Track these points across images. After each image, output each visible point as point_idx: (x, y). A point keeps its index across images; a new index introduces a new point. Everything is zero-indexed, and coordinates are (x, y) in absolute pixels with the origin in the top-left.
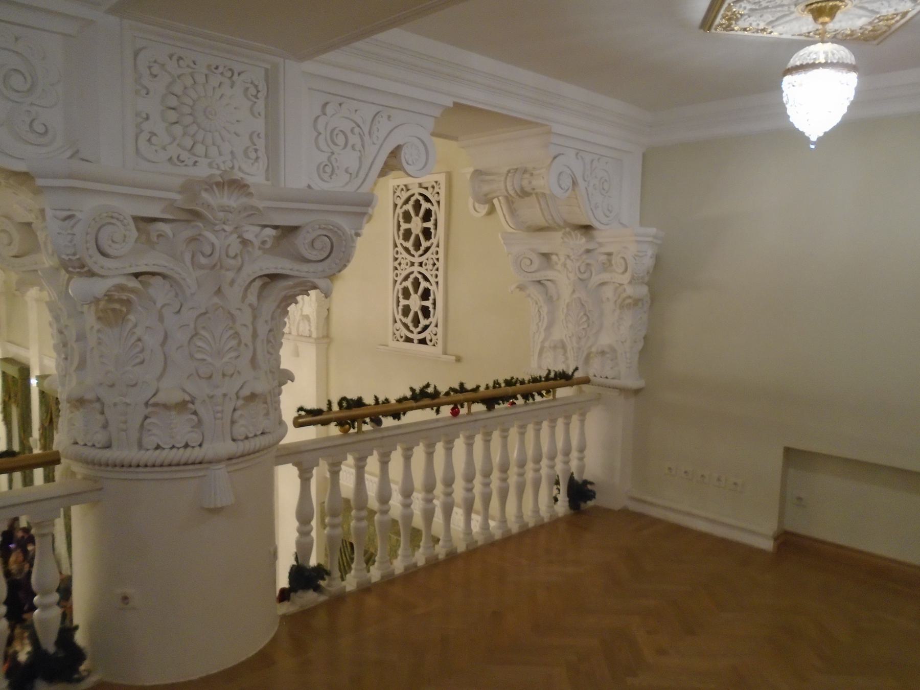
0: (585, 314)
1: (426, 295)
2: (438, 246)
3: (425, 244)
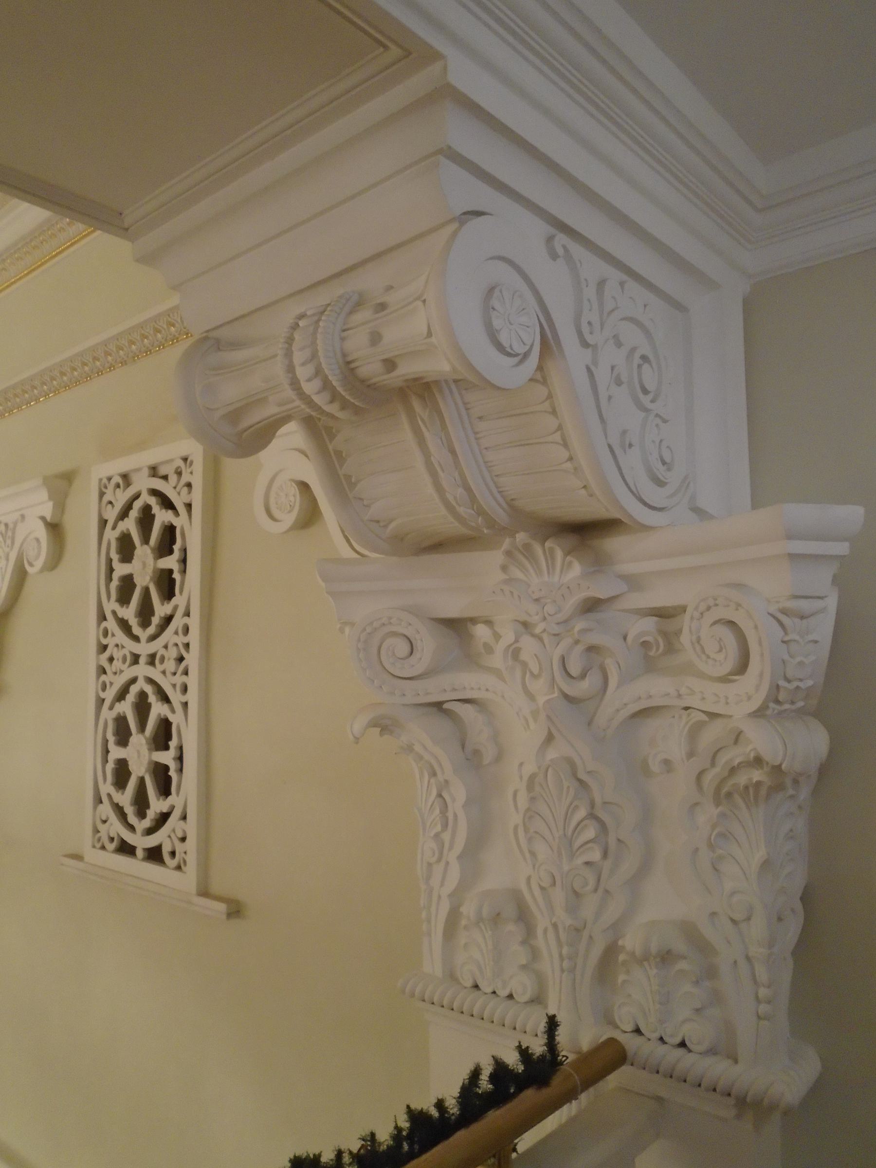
0: (592, 816)
1: (163, 735)
2: (187, 614)
3: (161, 609)
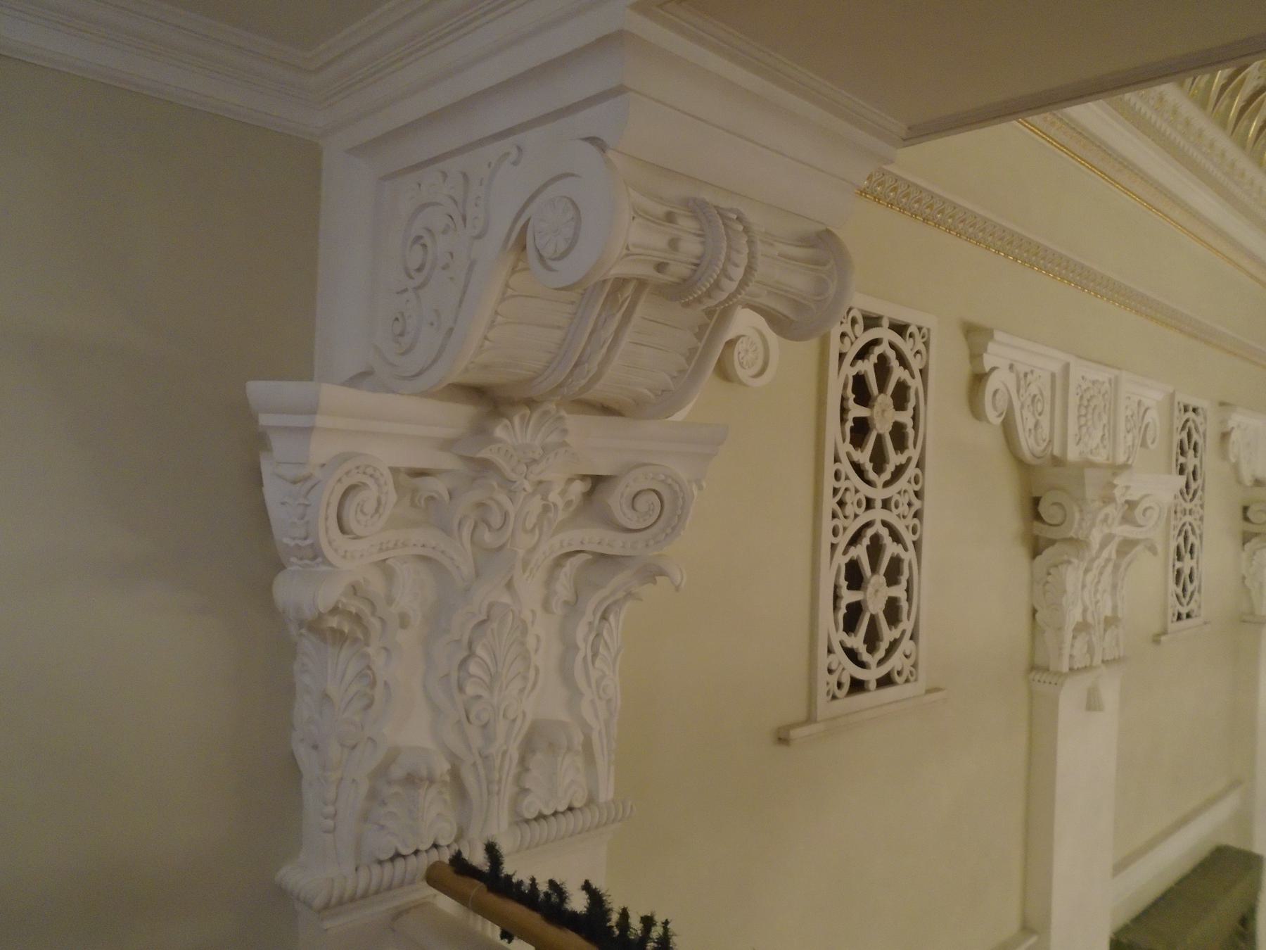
1: (861, 430)
2: (833, 546)
3: (860, 552)
